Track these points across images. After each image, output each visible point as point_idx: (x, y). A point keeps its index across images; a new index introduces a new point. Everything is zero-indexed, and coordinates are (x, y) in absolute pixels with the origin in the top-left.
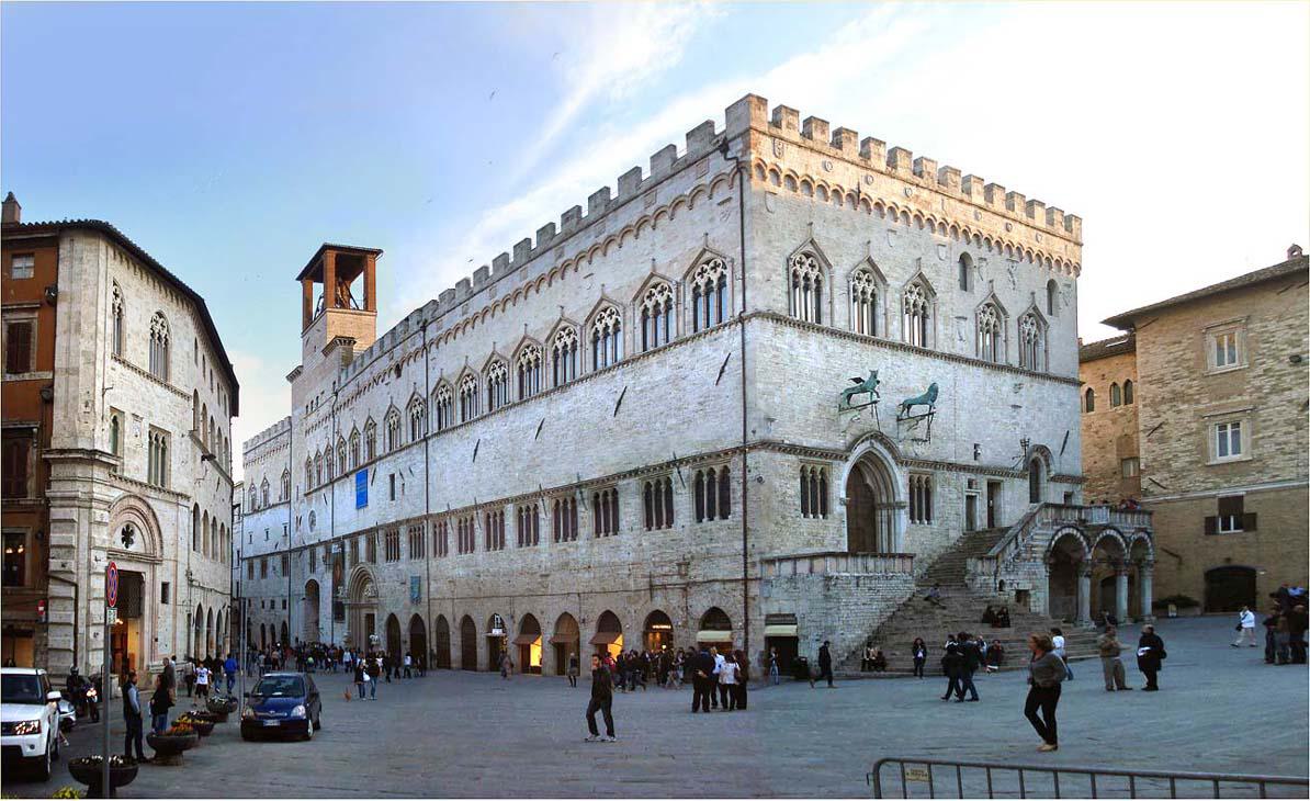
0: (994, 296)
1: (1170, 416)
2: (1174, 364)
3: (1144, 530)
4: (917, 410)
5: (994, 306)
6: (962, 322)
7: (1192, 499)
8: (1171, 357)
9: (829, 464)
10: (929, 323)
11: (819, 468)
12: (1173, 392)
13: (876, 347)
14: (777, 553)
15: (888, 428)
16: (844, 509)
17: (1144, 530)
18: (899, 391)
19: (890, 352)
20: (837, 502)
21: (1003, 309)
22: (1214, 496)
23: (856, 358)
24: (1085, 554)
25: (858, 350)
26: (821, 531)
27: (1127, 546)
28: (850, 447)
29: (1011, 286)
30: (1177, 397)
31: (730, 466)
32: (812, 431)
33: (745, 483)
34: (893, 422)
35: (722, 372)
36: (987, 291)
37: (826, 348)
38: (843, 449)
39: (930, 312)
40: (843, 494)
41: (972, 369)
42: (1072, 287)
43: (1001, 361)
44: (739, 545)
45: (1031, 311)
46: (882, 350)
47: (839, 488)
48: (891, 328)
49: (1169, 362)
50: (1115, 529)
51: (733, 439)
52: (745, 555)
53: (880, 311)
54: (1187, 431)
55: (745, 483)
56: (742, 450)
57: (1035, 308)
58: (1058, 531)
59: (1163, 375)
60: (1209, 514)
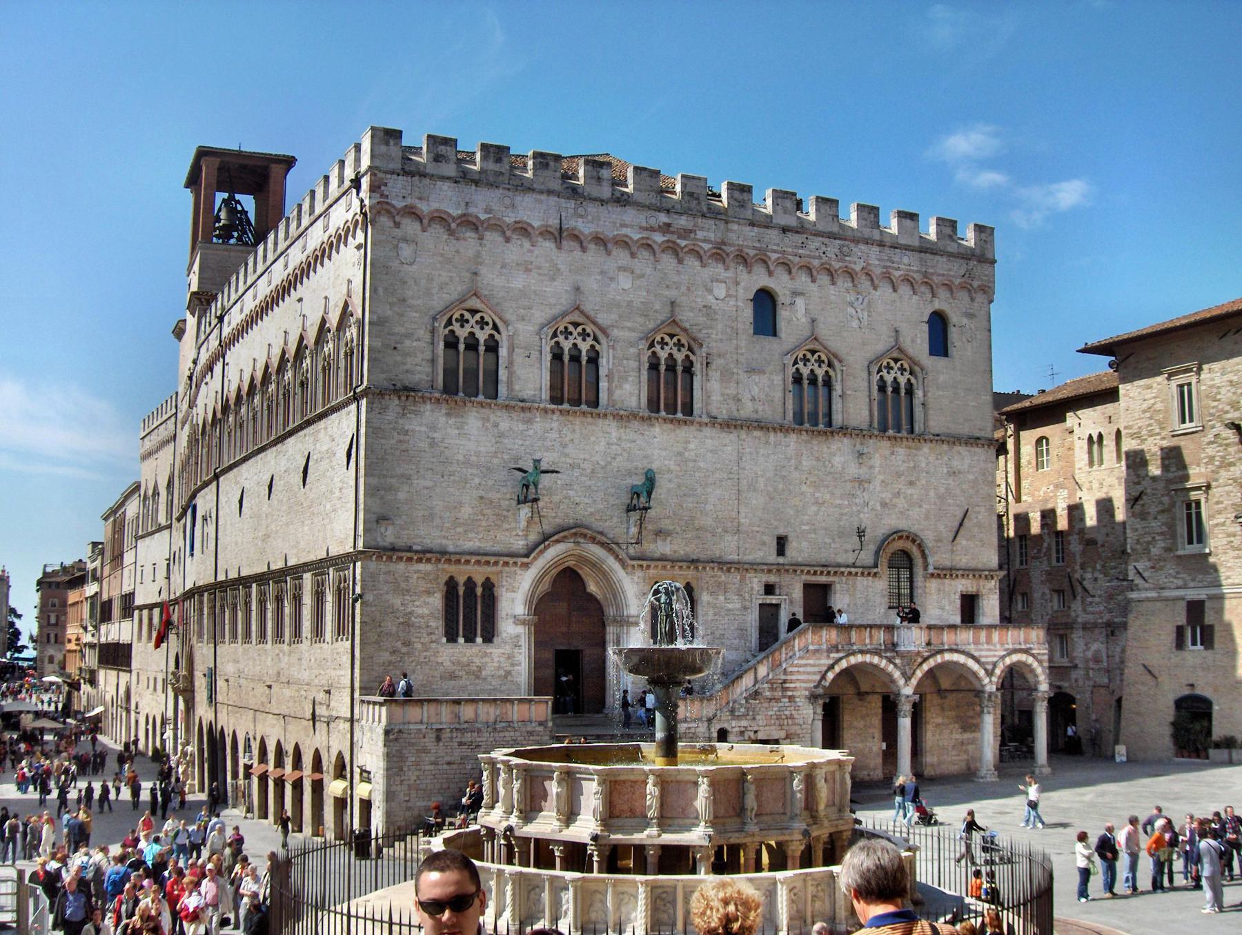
2: (1148, 415)
5: (814, 349)
7: (1167, 599)
8: (1145, 406)
11: (479, 580)
18: (630, 473)
19: (614, 424)
20: (511, 621)
23: (554, 435)
25: (555, 425)
26: (476, 660)
27: (990, 673)
28: (530, 551)
29: (855, 324)
37: (496, 425)
38: (522, 552)
39: (697, 368)
40: (520, 609)
45: (895, 355)
48: (618, 394)
49: (1144, 411)
50: (963, 652)
53: (603, 371)
54: (1160, 508)
57: (900, 350)
58: (841, 659)
59: (1140, 428)
60: (1180, 623)
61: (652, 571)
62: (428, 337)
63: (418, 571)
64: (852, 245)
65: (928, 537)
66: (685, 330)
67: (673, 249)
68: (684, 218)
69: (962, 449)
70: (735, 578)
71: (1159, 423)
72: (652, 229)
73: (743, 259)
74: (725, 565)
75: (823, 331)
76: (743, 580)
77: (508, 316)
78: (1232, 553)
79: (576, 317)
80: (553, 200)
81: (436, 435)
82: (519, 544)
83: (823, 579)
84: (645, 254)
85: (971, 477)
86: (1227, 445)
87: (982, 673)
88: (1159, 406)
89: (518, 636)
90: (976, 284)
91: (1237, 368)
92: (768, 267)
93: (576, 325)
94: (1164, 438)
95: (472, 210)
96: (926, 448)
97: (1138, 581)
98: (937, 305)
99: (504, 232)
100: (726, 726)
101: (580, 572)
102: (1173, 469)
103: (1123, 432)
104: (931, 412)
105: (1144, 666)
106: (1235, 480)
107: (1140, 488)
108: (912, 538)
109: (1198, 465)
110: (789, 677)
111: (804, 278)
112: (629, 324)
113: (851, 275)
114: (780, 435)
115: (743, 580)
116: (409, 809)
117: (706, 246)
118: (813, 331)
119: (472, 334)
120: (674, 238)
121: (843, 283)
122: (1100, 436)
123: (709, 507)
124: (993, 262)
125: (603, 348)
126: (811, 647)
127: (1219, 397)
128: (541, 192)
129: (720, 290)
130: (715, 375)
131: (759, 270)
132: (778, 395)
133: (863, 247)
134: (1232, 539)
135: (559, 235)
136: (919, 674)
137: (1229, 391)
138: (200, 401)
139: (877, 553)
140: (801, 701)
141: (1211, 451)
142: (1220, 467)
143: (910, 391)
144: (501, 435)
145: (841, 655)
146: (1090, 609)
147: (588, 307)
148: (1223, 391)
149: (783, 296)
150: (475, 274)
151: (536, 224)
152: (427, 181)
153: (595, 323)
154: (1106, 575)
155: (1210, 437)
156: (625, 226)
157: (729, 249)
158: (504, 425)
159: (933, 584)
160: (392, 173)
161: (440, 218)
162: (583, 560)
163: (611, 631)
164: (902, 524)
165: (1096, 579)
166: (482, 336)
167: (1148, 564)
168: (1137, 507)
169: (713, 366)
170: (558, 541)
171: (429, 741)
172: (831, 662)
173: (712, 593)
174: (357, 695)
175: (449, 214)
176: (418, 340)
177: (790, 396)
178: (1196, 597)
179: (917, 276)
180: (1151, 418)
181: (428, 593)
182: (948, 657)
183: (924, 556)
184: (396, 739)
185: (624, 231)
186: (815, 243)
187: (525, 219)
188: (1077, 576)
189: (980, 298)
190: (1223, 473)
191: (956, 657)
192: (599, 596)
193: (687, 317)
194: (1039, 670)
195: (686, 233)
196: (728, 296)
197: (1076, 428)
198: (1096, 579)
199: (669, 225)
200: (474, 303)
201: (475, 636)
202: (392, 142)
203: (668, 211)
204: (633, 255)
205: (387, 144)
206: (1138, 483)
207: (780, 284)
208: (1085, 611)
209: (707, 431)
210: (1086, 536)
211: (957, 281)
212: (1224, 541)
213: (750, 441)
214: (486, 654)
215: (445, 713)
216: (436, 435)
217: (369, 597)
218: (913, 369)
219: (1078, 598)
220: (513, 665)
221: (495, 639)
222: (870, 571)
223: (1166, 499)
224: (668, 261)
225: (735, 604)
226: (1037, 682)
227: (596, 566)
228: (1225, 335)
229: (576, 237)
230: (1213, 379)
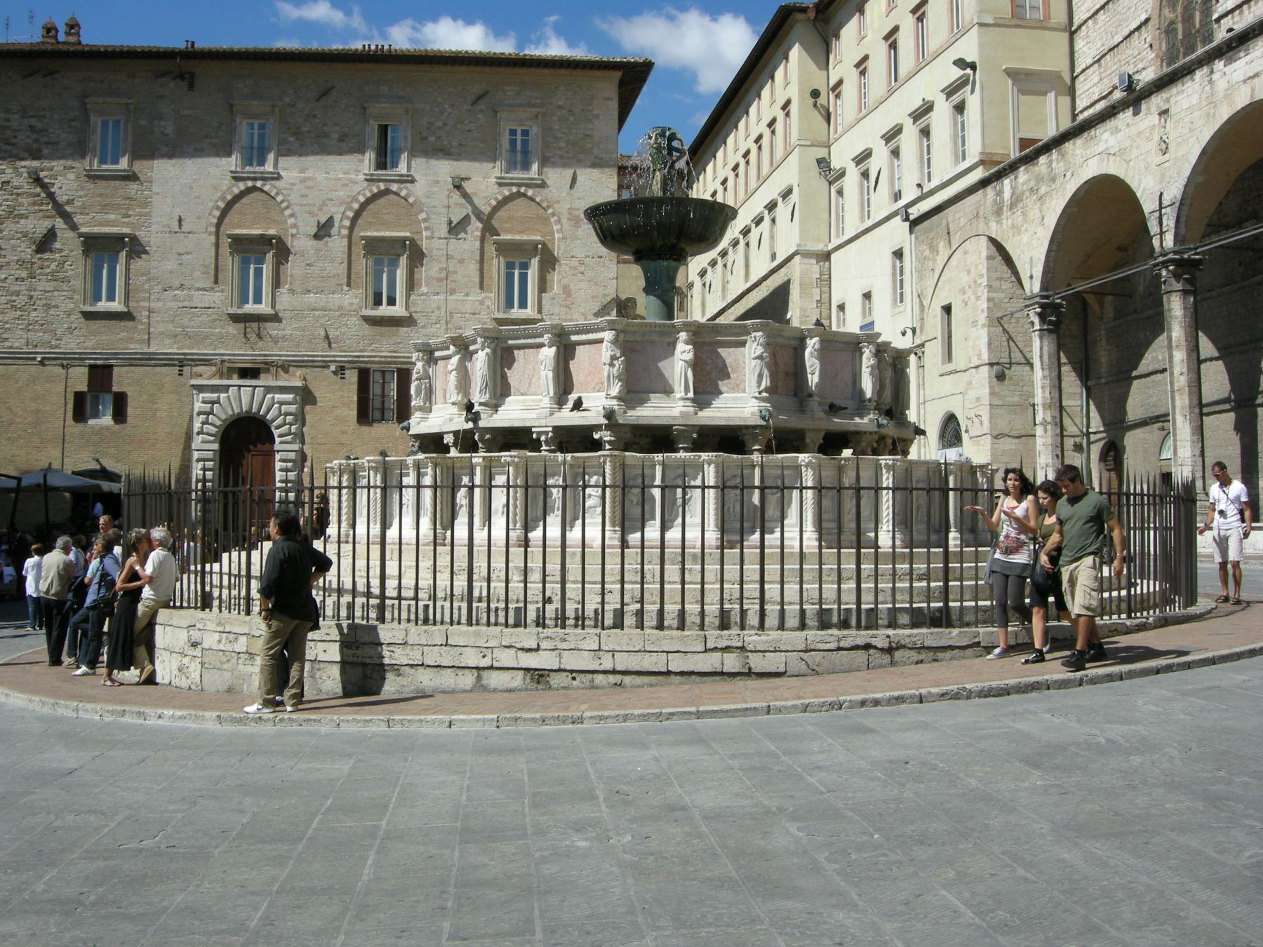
91: (42, 113)
106: (25, 235)
127: (14, 141)
134: (14, 298)
137: (28, 136)
228: (32, 75)
230: (8, 120)
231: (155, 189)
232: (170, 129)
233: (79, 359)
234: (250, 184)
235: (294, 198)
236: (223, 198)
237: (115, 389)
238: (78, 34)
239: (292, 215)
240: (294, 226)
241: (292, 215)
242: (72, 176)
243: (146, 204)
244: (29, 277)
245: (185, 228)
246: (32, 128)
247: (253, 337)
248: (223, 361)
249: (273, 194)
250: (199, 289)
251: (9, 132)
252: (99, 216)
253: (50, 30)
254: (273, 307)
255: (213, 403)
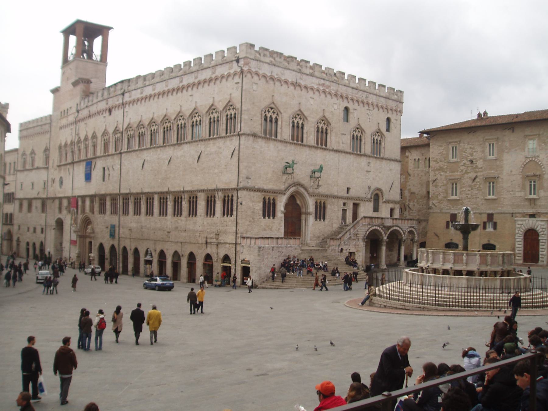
0: (359, 124)
1: (438, 176)
2: (440, 155)
3: (413, 227)
4: (317, 175)
5: (359, 128)
6: (343, 136)
8: (439, 152)
9: (277, 196)
10: (328, 136)
11: (272, 198)
12: (440, 166)
13: (301, 147)
14: (248, 235)
15: (306, 181)
16: (283, 215)
17: (413, 227)
20: (280, 212)
21: (363, 130)
22: (449, 213)
24: (383, 238)
25: (293, 148)
27: (404, 234)
28: (287, 189)
29: (368, 120)
30: (441, 169)
31: (234, 195)
32: (269, 182)
33: (237, 203)
34: (308, 178)
35: (232, 154)
36: (357, 123)
37: (278, 147)
39: (329, 131)
40: (282, 209)
41: (348, 156)
42: (398, 120)
43: (362, 153)
44: (234, 229)
45: (378, 131)
46: (304, 148)
47: (281, 207)
48: (309, 139)
49: (439, 154)
50: (399, 227)
51: (234, 186)
52: (236, 233)
53: (305, 131)
54: (442, 184)
55: (237, 203)
56: (237, 190)
57: (379, 129)
58: (370, 228)
61: (316, 197)
62: (260, 116)
63: (257, 195)
64: (369, 94)
65: (383, 189)
66: (327, 119)
67: (324, 92)
68: (328, 82)
69: (392, 162)
70: (336, 200)
71: (444, 158)
72: (319, 84)
73: (342, 96)
74: (335, 197)
75: (361, 123)
76: (338, 201)
77: (282, 111)
78: (467, 200)
79: (299, 113)
80: (294, 73)
81: (262, 150)
82: (283, 187)
83: (357, 202)
84: (317, 93)
85: (394, 171)
86: (468, 167)
87: (403, 233)
88: (444, 152)
89: (282, 217)
90: (399, 109)
92: (348, 100)
93: (298, 115)
94: (445, 163)
95: (273, 74)
96: (384, 161)
97: (433, 206)
98: (389, 115)
99: (281, 82)
100: (343, 247)
101: (296, 197)
102: (448, 172)
103: (431, 159)
104: (385, 150)
105: (435, 233)
106: (470, 178)
107: (435, 178)
108: (379, 190)
109: (457, 172)
110: (358, 233)
111: (356, 104)
112: (312, 116)
113: (368, 104)
114: (349, 155)
115: (338, 201)
116: (265, 272)
117: (333, 92)
118: (358, 122)
119: (271, 116)
120: (325, 88)
121: (366, 107)
122: (419, 159)
123: (331, 177)
124: (403, 103)
125: (305, 123)
126: (364, 223)
128: (291, 70)
129: (336, 107)
130: (333, 134)
131: (346, 101)
132: (349, 142)
133: (372, 95)
135: (295, 85)
136: (388, 233)
138: (92, 122)
139: (371, 194)
140: (361, 240)
141: (462, 168)
142: (465, 173)
143: (380, 144)
144: (279, 151)
145: (371, 226)
146: (411, 214)
147: (302, 110)
148: (468, 150)
149: (351, 110)
150: (273, 96)
151: (290, 80)
152: (261, 63)
153: (304, 115)
154: (418, 204)
155: (462, 164)
156: (313, 83)
157: (339, 93)
158: (280, 148)
159: (384, 205)
160: (252, 59)
161: (264, 76)
162: (297, 192)
163: (303, 217)
164: (378, 186)
165: (414, 205)
166: (274, 117)
167: (437, 201)
168: (434, 183)
169: (333, 131)
170: (293, 186)
171: (270, 251)
172: (368, 228)
173: (331, 205)
174: (239, 235)
175: (267, 75)
176: (258, 117)
177: (352, 142)
178: (454, 213)
179: (385, 106)
180: (441, 156)
181: (259, 202)
182: (393, 229)
183: (383, 196)
184: (262, 250)
185: (313, 85)
186: (360, 93)
187: (287, 78)
188: (407, 203)
189: (399, 114)
190: (466, 176)
191: (397, 228)
192: (300, 204)
193: (327, 115)
194: (416, 233)
195: (328, 87)
196: (338, 109)
197: (409, 156)
198: (414, 205)
199: (324, 84)
200: (272, 106)
201: (270, 216)
202: (252, 48)
203: (324, 79)
204: (314, 93)
205: (251, 49)
206: (435, 176)
207: (351, 106)
208: (409, 215)
209: (331, 153)
210: (412, 191)
211: (394, 108)
212: (465, 196)
213: (342, 156)
214: (274, 223)
215: (274, 240)
216: (262, 150)
217: (243, 203)
218: (382, 135)
219: (407, 211)
220: (280, 226)
221: (275, 217)
222: (369, 200)
223: (445, 182)
224: (323, 95)
225: (336, 209)
226: (415, 237)
227: (301, 195)
229: (299, 86)
231: (504, 163)
232: (508, 145)
233: (485, 213)
234: (531, 159)
235: (544, 163)
236: (523, 164)
237: (494, 221)
238: (487, 115)
239: (544, 168)
240: (544, 171)
241: (544, 168)
242: (481, 160)
243: (502, 167)
244: (472, 189)
245: (513, 173)
246: (471, 148)
247: (533, 205)
248: (524, 213)
249: (538, 161)
250: (517, 191)
251: (465, 150)
252: (489, 171)
253: (479, 115)
254: (538, 196)
255: (521, 225)
